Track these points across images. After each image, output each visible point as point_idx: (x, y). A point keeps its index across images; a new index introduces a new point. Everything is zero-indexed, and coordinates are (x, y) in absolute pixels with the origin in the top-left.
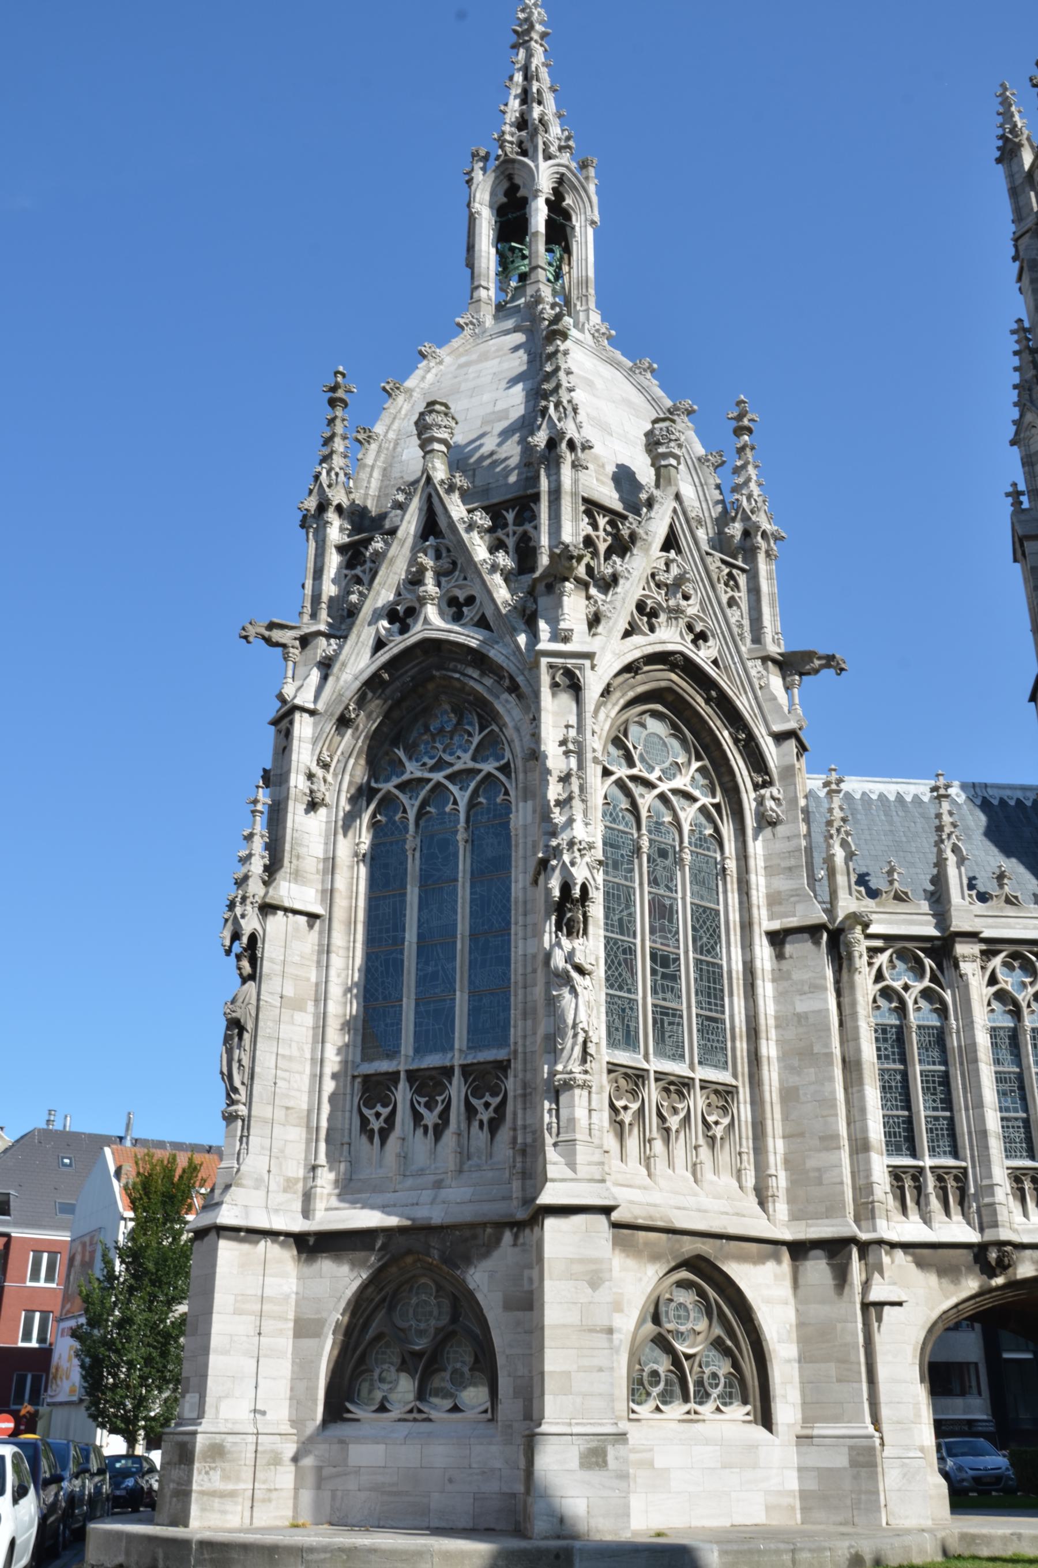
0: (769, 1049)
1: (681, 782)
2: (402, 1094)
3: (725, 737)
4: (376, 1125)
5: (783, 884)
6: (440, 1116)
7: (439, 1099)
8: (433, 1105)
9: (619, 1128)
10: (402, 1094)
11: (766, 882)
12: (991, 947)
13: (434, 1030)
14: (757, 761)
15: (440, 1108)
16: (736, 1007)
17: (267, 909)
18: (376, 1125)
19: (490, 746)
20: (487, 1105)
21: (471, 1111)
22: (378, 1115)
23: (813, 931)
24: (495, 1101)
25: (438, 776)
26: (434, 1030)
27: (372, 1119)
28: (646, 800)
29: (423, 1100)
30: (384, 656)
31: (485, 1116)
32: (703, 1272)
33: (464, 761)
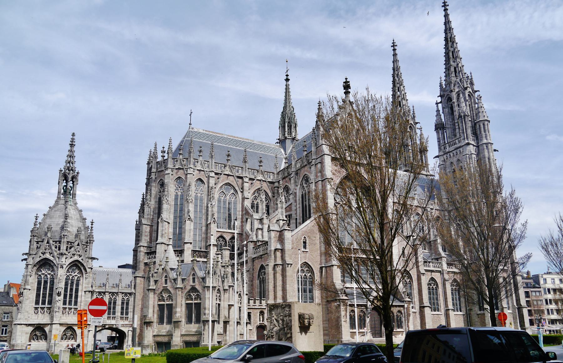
0: (82, 304)
1: (76, 274)
3: (82, 268)
5: (87, 286)
9: (63, 313)
11: (85, 284)
12: (110, 293)
13: (44, 303)
14: (86, 271)
16: (79, 299)
17: (24, 289)
19: (53, 271)
23: (89, 291)
26: (44, 303)
28: (71, 277)
30: (41, 258)
32: (70, 328)
33: (49, 272)
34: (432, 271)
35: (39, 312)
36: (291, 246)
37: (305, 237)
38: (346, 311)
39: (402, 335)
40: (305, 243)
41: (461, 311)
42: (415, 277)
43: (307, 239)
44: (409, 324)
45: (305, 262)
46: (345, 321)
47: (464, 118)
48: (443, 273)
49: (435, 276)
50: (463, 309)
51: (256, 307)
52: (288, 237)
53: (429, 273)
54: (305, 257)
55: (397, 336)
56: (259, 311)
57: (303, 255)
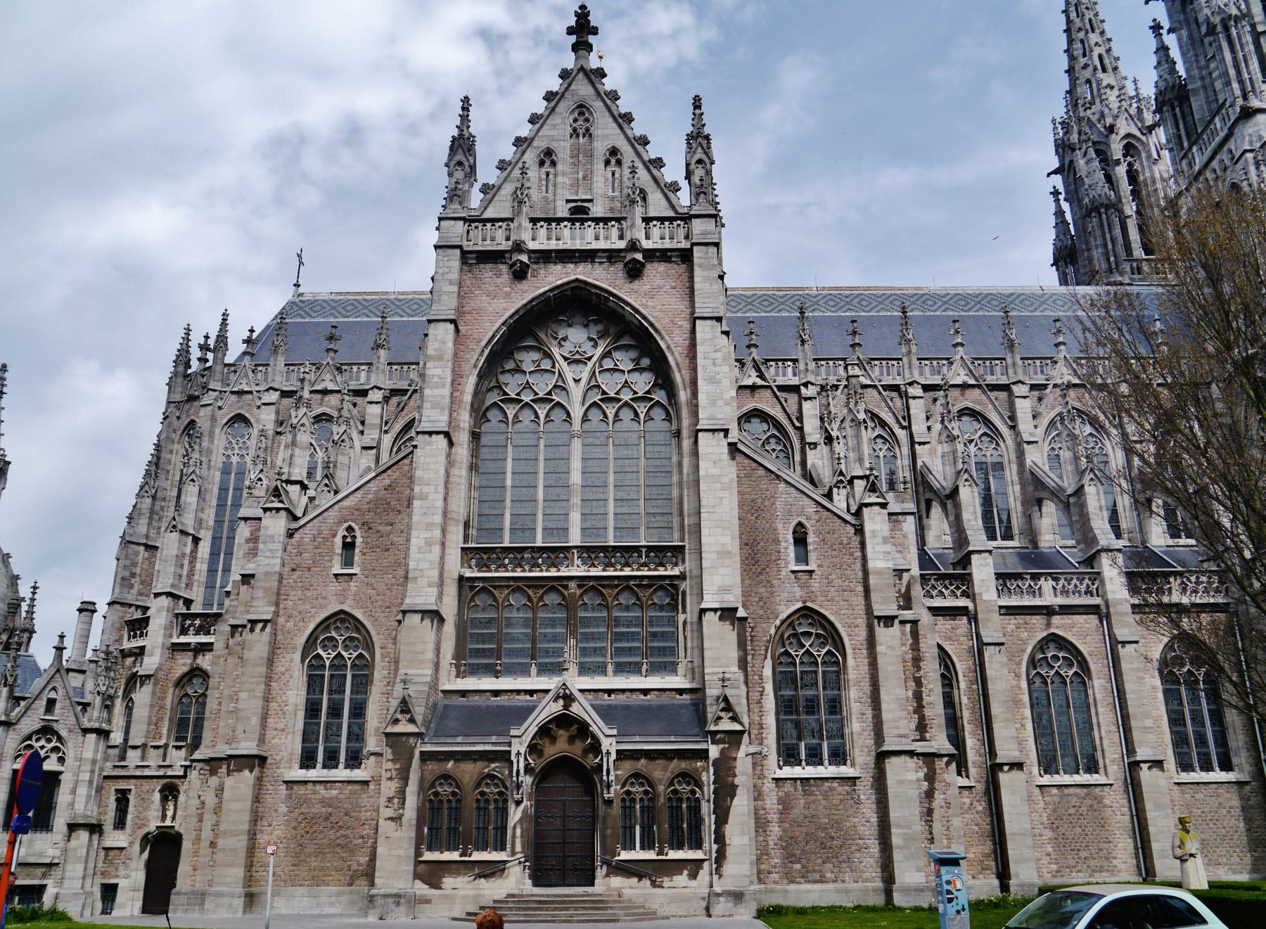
34: (1048, 611)
36: (278, 561)
37: (350, 529)
38: (405, 779)
39: (693, 876)
40: (349, 546)
41: (1226, 766)
42: (853, 638)
43: (358, 534)
44: (730, 830)
45: (342, 612)
46: (397, 819)
47: (1227, 29)
48: (1108, 616)
49: (1072, 627)
50: (1241, 758)
51: (147, 772)
52: (271, 531)
53: (1037, 620)
54: (342, 596)
55: (666, 881)
56: (158, 785)
57: (334, 587)
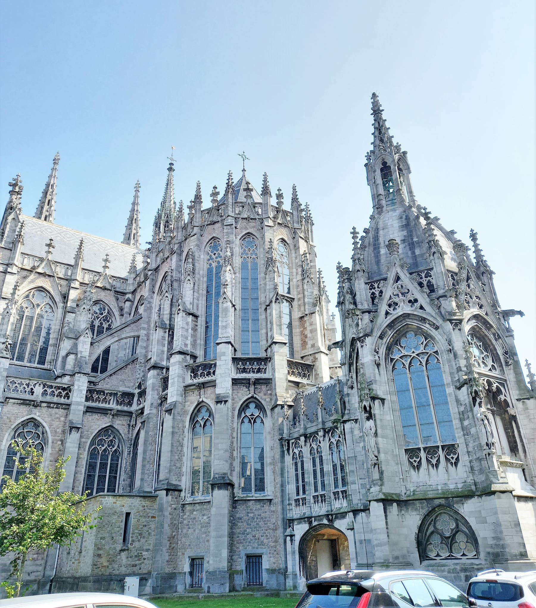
2: (423, 454)
4: (416, 464)
6: (437, 461)
7: (436, 456)
8: (433, 458)
10: (423, 454)
15: (436, 459)
18: (416, 464)
20: (452, 458)
21: (447, 459)
22: (415, 461)
24: (455, 457)
25: (414, 355)
27: (414, 463)
29: (430, 456)
31: (453, 461)
35: (424, 461)
